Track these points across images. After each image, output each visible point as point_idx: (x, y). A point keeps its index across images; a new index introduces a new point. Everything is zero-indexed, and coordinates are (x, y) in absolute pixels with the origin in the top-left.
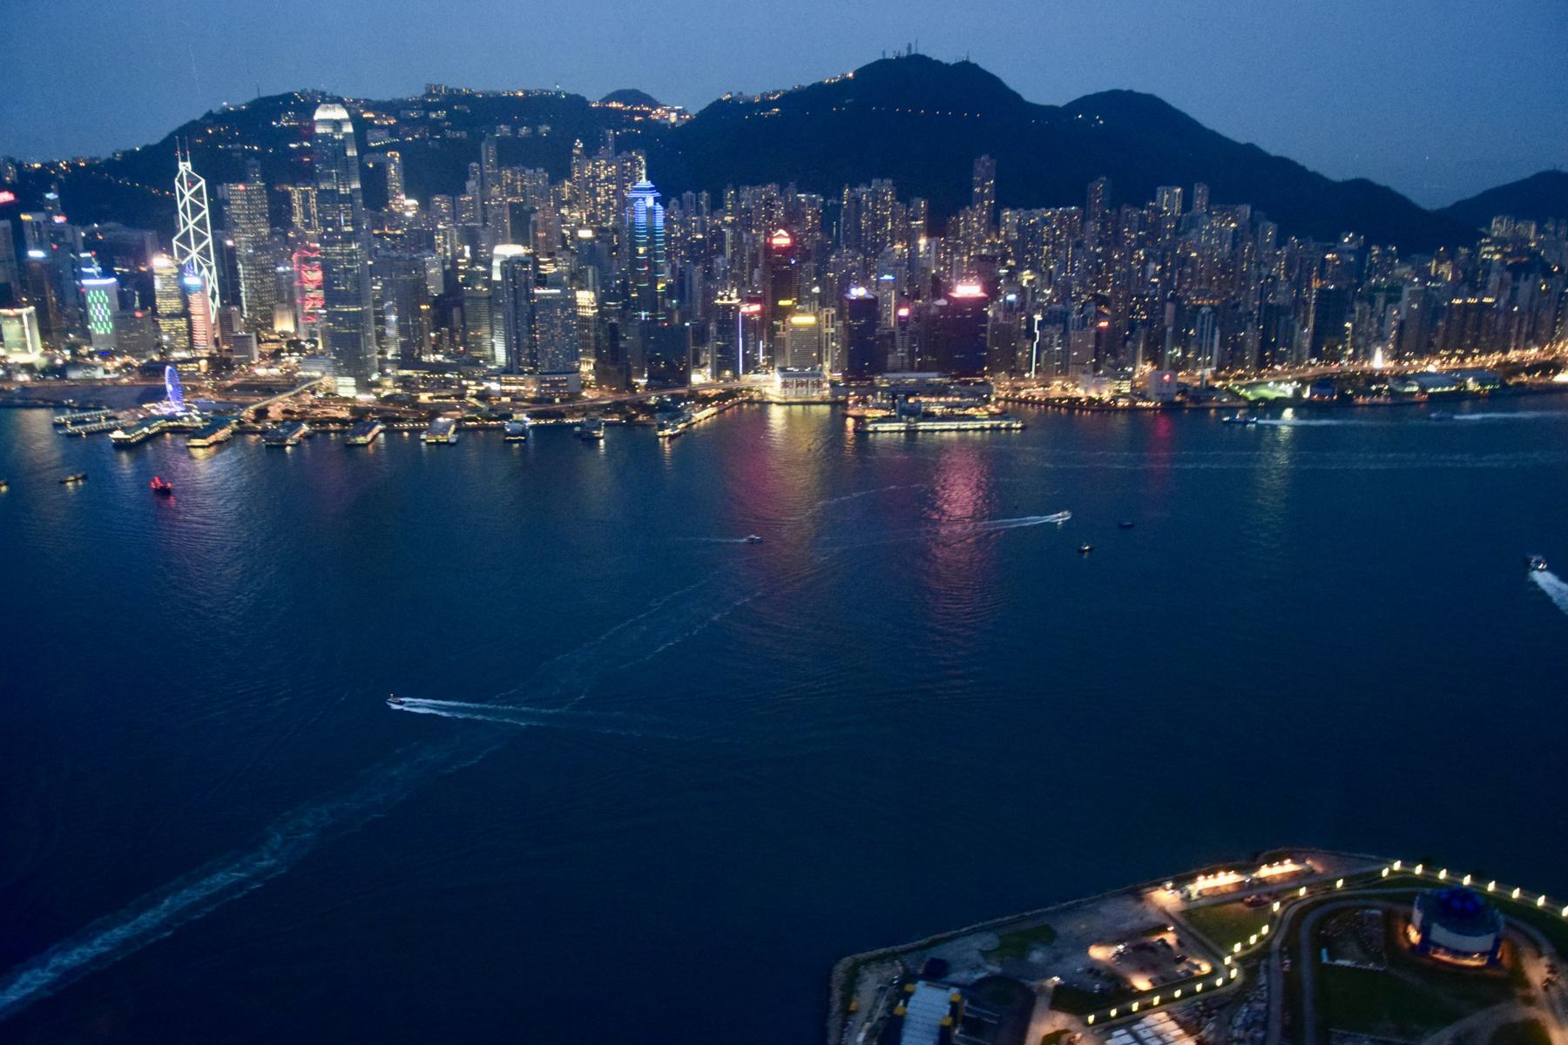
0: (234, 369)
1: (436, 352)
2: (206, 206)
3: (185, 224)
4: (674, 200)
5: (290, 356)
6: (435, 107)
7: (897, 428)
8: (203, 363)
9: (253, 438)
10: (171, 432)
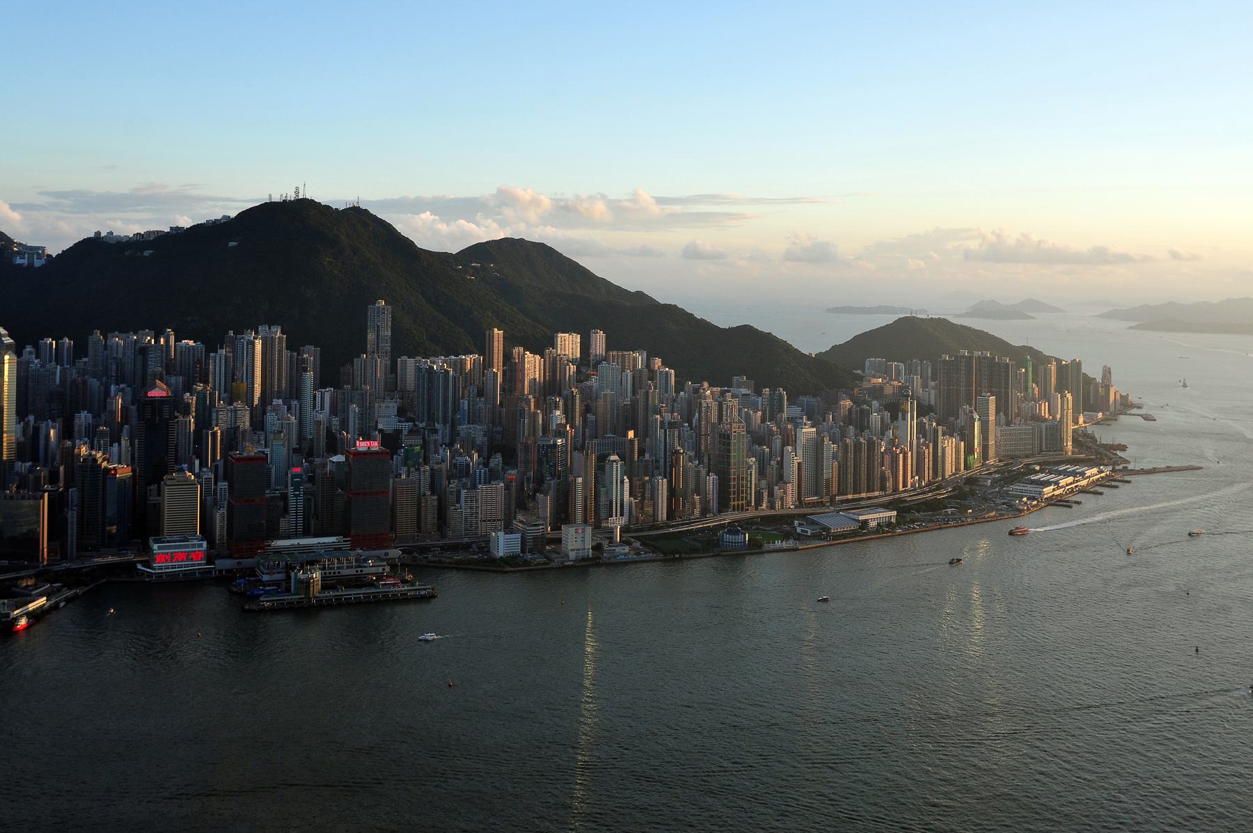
4: (29, 348)
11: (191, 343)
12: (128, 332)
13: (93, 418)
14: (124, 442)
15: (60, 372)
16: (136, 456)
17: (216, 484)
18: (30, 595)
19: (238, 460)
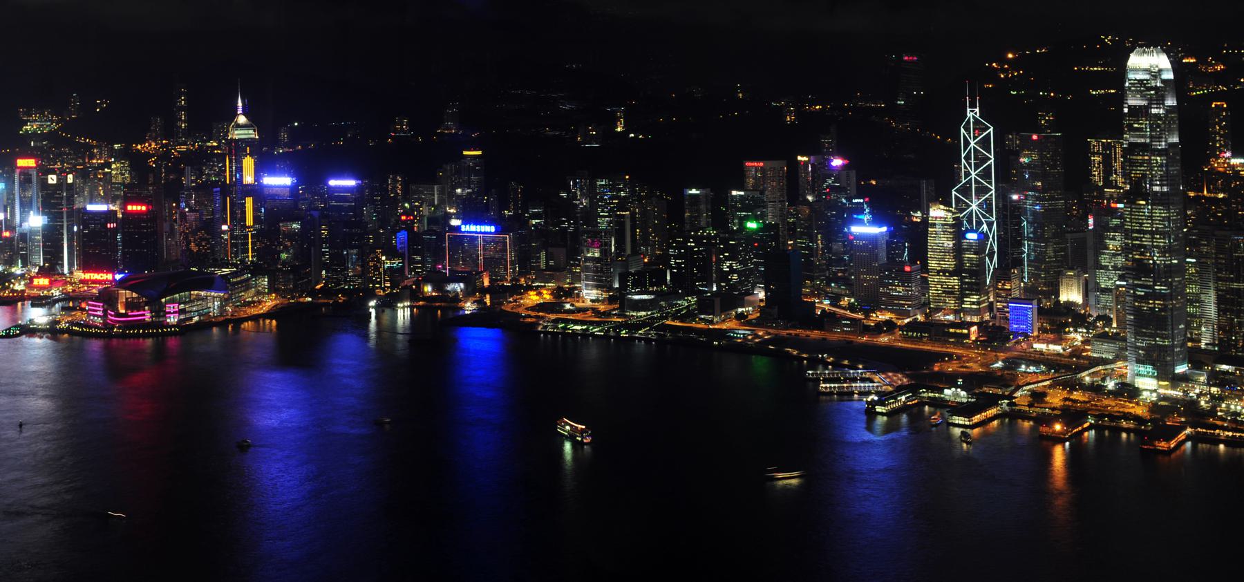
2: (992, 157)
3: (967, 174)
5: (1076, 331)
8: (974, 329)
9: (1027, 425)
10: (930, 406)
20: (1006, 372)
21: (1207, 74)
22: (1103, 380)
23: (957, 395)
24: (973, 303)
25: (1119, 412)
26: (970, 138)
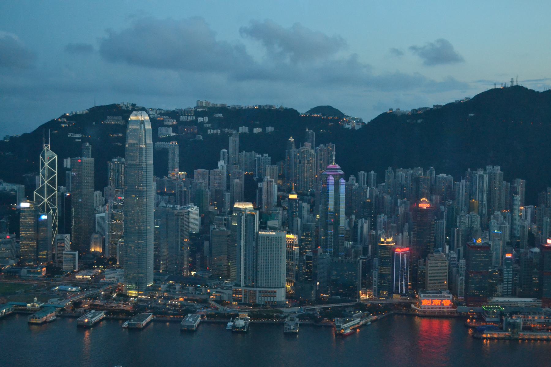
0: (62, 273)
1: (191, 270)
2: (57, 172)
3: (43, 182)
4: (352, 177)
5: (98, 268)
6: (202, 114)
7: (503, 336)
11: (445, 175)
12: (408, 168)
13: (388, 218)
14: (406, 234)
15: (369, 191)
16: (412, 240)
17: (458, 261)
18: (351, 317)
19: (472, 247)
20: (60, 292)
21: (168, 126)
22: (111, 293)
23: (33, 306)
24: (44, 255)
25: (118, 309)
26: (45, 162)
